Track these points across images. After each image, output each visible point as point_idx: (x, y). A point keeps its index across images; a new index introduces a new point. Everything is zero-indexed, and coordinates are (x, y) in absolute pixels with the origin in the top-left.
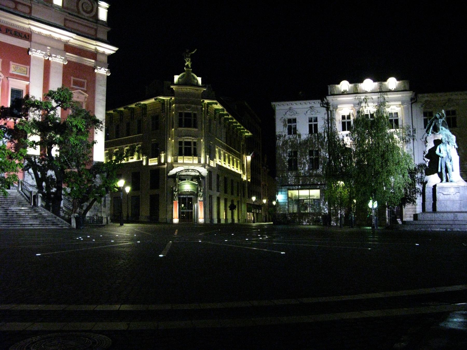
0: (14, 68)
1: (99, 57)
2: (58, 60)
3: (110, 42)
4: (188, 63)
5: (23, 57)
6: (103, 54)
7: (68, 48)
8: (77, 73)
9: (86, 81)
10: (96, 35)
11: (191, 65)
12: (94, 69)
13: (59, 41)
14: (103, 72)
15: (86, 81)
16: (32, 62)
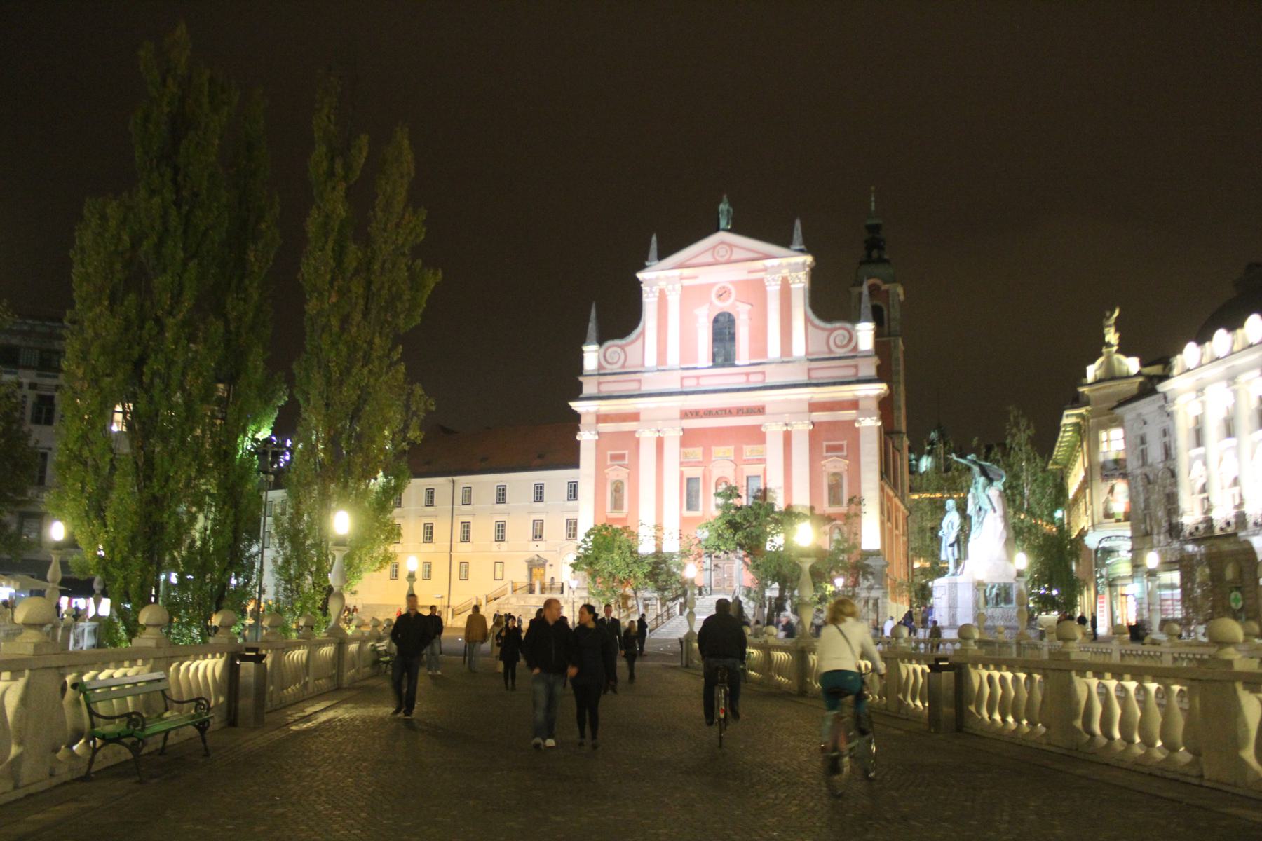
0: (749, 451)
1: (861, 404)
2: (802, 428)
3: (879, 379)
4: (1112, 336)
5: (757, 435)
6: (867, 397)
7: (815, 407)
8: (830, 437)
9: (845, 443)
10: (856, 374)
11: (1120, 338)
12: (854, 421)
13: (800, 401)
14: (870, 423)
15: (845, 443)
16: (769, 438)
